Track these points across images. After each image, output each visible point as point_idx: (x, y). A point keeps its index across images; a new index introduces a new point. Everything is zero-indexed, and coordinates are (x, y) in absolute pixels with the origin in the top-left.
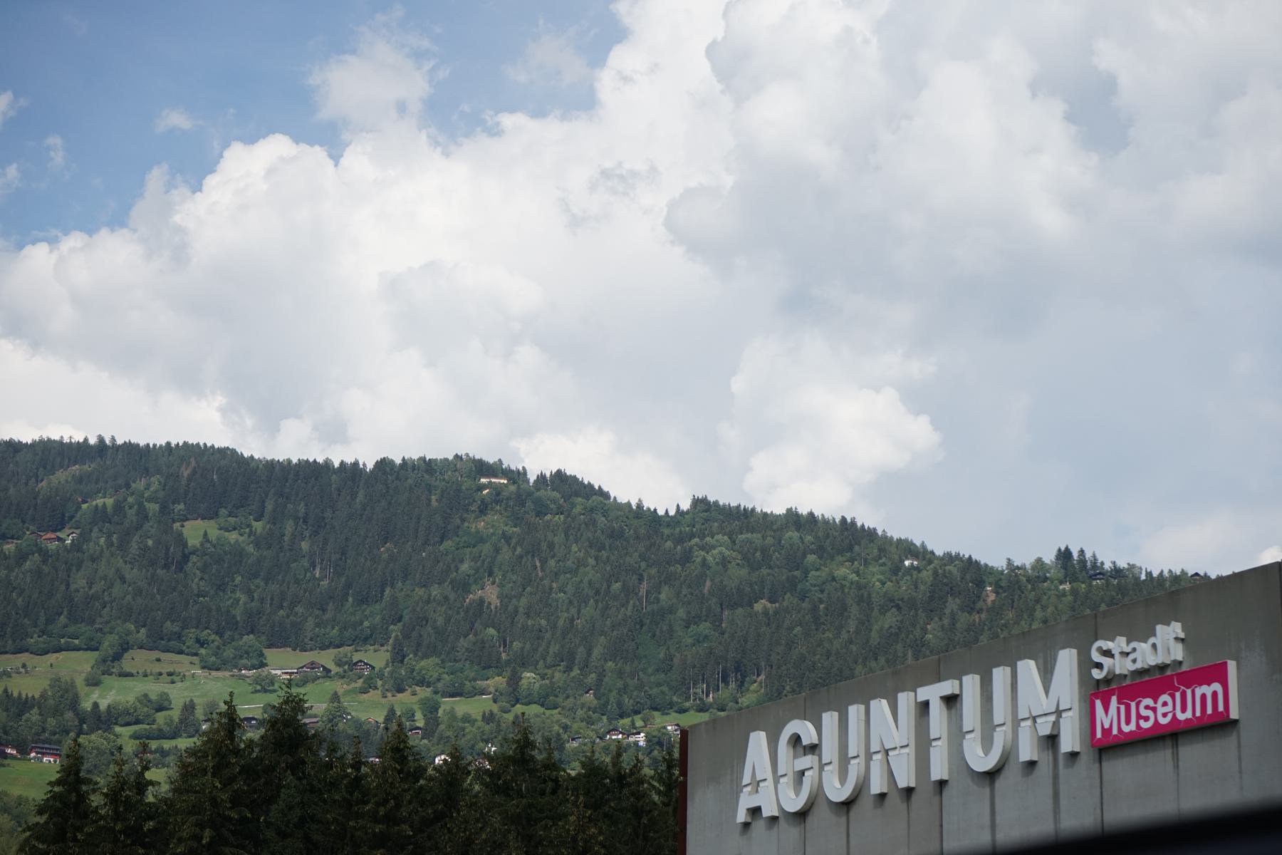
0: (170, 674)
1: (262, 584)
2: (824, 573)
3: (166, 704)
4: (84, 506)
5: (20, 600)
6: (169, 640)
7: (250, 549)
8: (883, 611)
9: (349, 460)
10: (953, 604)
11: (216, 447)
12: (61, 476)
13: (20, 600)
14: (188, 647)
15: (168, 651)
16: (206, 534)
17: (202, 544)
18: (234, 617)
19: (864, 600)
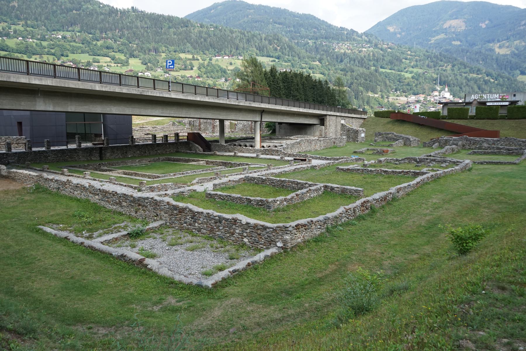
2: (86, 6)
8: (101, 15)
10: (113, 15)
19: (96, 13)
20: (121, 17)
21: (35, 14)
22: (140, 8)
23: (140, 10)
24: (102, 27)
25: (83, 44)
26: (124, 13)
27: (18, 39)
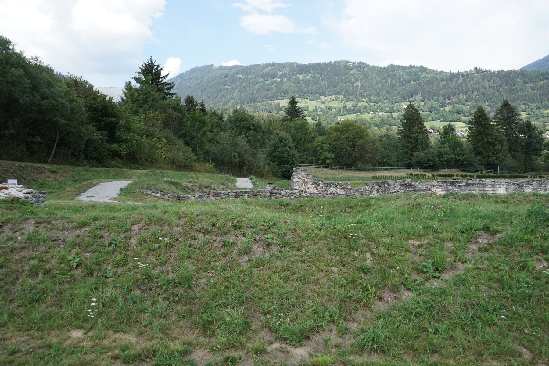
8: (442, 81)
9: (324, 62)
10: (455, 79)
19: (437, 79)
20: (464, 80)
21: (376, 90)
22: (485, 67)
23: (484, 70)
24: (446, 93)
25: (431, 112)
26: (466, 76)
27: (369, 113)
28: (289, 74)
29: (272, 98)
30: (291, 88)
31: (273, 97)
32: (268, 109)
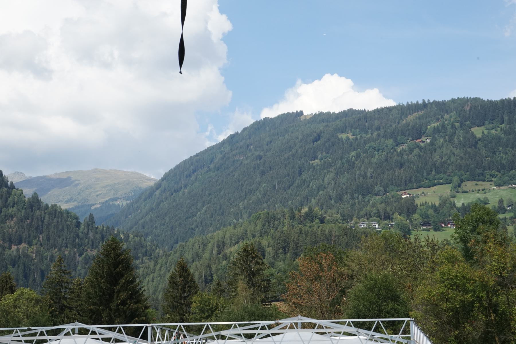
0: (483, 190)
1: (511, 149)
3: (487, 201)
4: (429, 127)
5: (415, 167)
6: (479, 176)
7: (503, 136)
11: (472, 98)
12: (410, 118)
13: (415, 167)
14: (488, 178)
15: (479, 181)
16: (483, 132)
17: (482, 136)
18: (503, 164)
28: (453, 126)
29: (407, 185)
30: (453, 159)
31: (410, 181)
32: (381, 211)
